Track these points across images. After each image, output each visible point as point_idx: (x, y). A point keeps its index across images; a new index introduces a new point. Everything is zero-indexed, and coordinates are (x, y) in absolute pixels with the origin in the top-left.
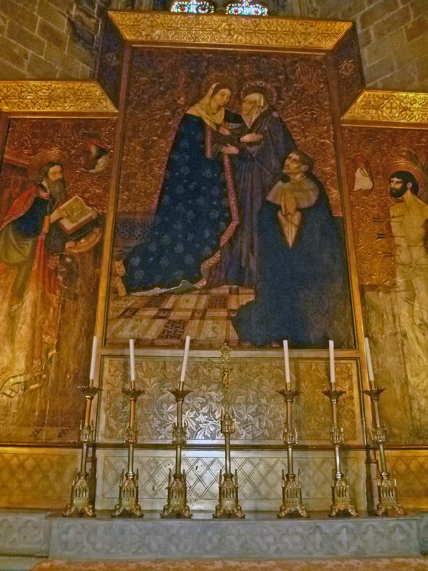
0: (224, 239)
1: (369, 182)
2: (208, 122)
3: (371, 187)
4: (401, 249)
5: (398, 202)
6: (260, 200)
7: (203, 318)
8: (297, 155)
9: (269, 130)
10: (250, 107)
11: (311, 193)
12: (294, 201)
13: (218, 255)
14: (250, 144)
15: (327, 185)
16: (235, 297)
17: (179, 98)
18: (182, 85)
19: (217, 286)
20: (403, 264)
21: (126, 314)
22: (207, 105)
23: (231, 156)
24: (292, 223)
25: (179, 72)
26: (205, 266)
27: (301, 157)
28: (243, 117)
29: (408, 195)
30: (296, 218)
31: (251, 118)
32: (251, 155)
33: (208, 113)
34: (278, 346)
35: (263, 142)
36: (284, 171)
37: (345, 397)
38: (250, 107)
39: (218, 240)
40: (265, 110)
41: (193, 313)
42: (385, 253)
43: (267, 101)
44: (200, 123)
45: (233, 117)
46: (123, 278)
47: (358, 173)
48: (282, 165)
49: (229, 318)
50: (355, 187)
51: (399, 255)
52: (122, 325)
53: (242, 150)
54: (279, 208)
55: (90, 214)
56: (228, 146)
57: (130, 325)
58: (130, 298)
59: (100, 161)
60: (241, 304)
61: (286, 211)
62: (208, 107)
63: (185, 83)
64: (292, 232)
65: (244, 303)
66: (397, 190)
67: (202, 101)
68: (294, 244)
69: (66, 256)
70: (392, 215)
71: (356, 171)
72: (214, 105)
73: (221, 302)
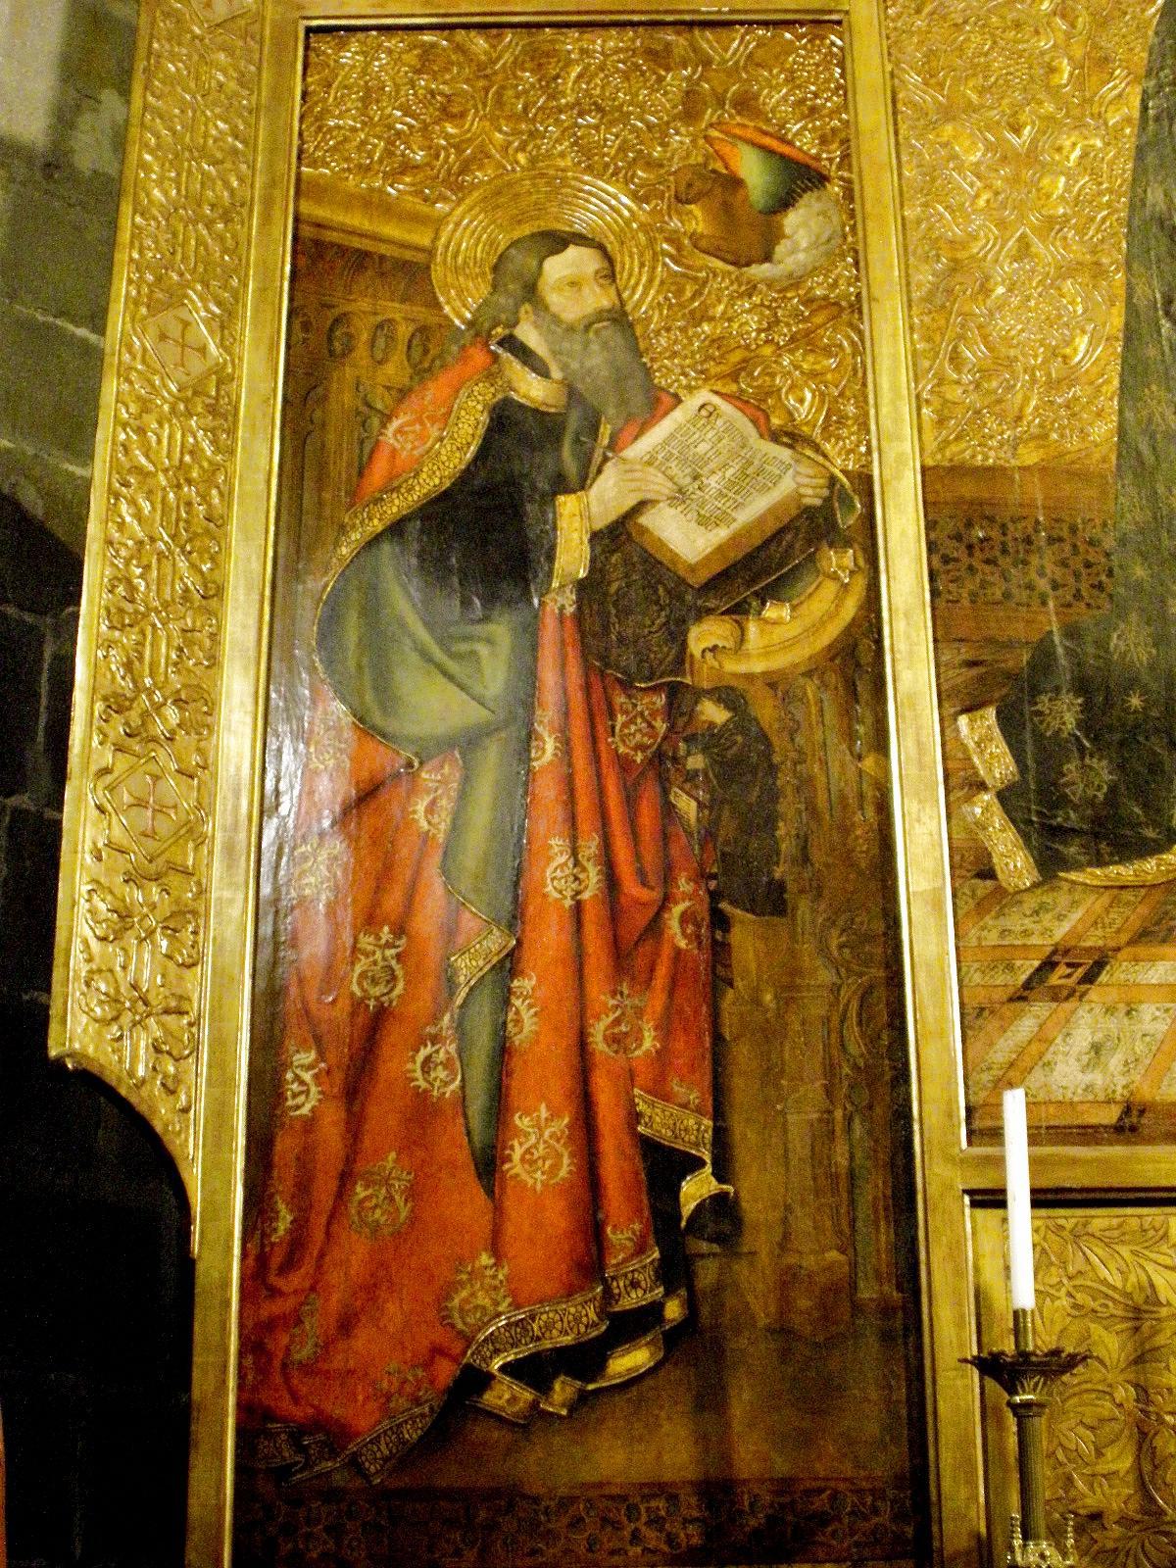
21: (1055, 979)
46: (1002, 797)
52: (1042, 1038)
55: (786, 486)
57: (1083, 1036)
58: (1063, 899)
59: (791, 220)
69: (699, 694)
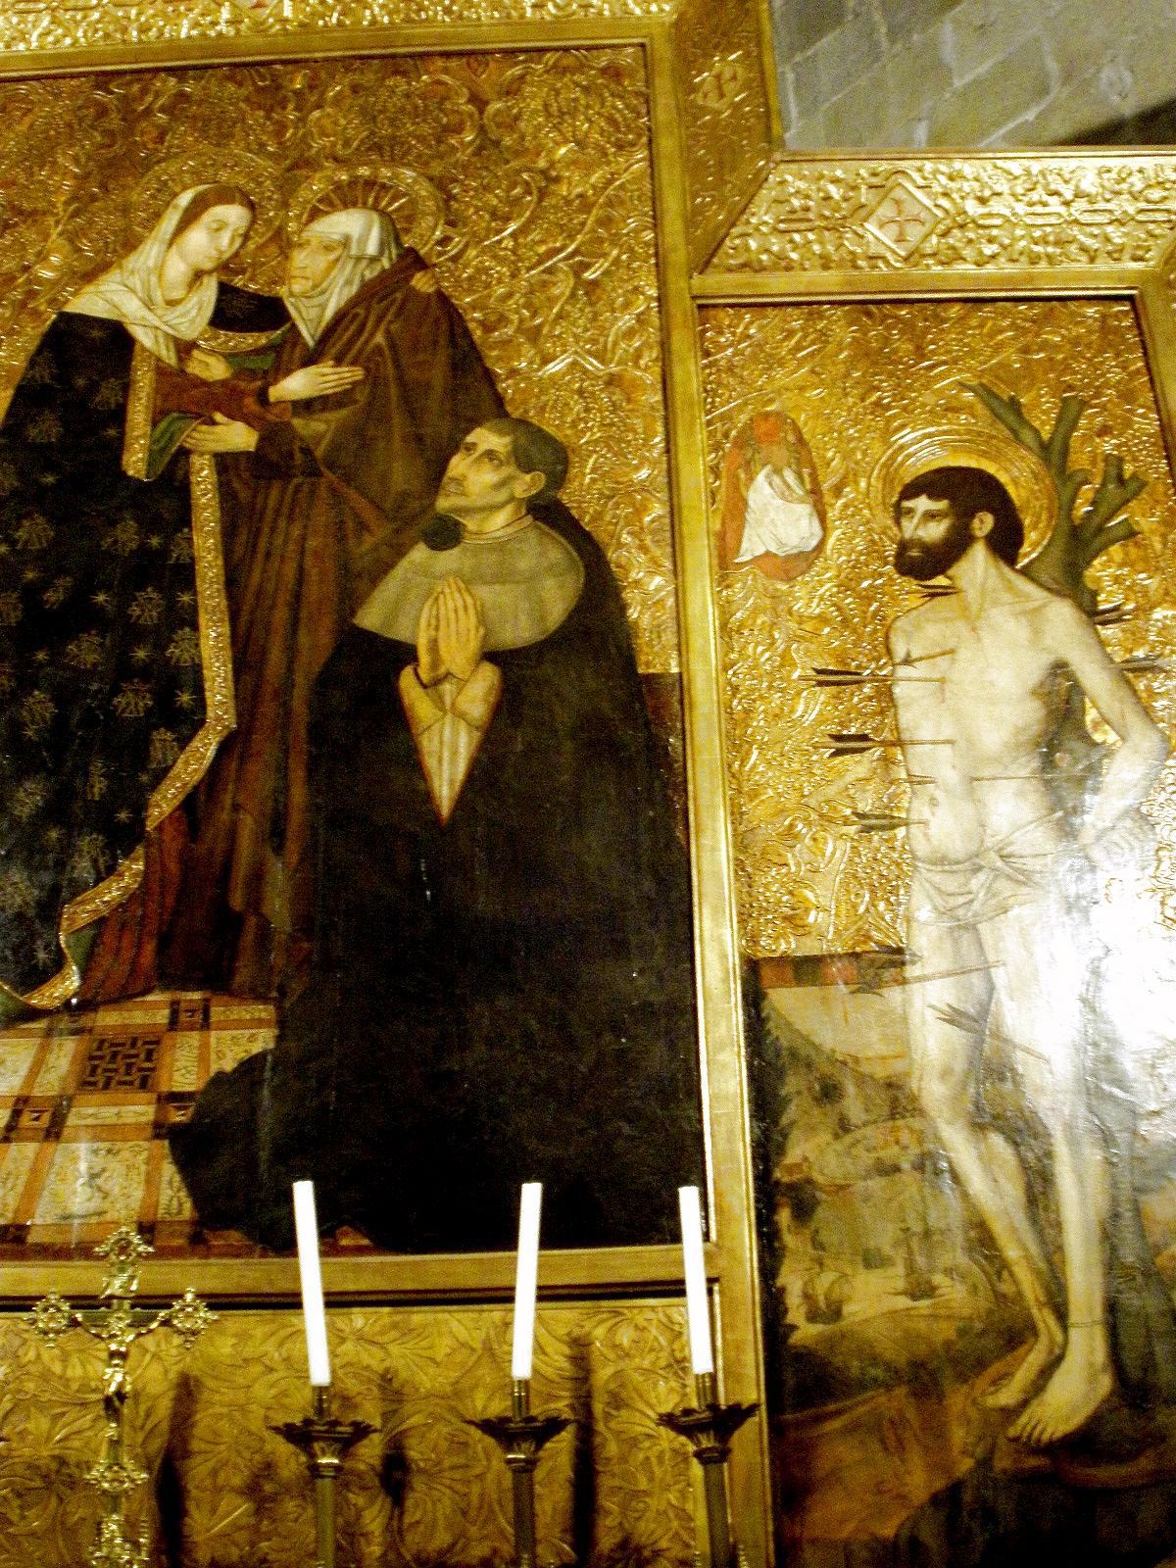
0: (163, 803)
1: (804, 522)
2: (143, 337)
3: (814, 543)
4: (939, 794)
5: (933, 596)
6: (327, 623)
7: (54, 1132)
8: (501, 433)
9: (393, 346)
10: (323, 261)
11: (550, 583)
12: (473, 620)
13: (133, 868)
14: (306, 406)
15: (620, 545)
16: (194, 1038)
17: (42, 257)
18: (60, 208)
19: (123, 996)
20: (941, 861)
22: (149, 271)
23: (225, 463)
24: (461, 715)
25: (54, 163)
26: (79, 914)
27: (515, 442)
28: (289, 304)
29: (977, 565)
30: (478, 692)
31: (323, 307)
32: (307, 451)
33: (149, 304)
34: (365, 1242)
35: (361, 397)
36: (443, 504)
37: (653, 1454)
38: (323, 261)
39: (140, 808)
40: (384, 271)
41: (16, 1114)
42: (862, 816)
43: (393, 231)
44: (116, 339)
45: (246, 308)
47: (762, 492)
48: (436, 474)
49: (160, 1129)
50: (745, 545)
51: (924, 823)
53: (273, 434)
54: (406, 654)
56: (214, 423)
60: (214, 1068)
61: (435, 663)
62: (154, 279)
63: (75, 198)
64: (454, 753)
65: (229, 1065)
66: (926, 548)
67: (133, 261)
68: (462, 801)
70: (900, 652)
71: (751, 479)
72: (177, 269)
73: (118, 1065)
